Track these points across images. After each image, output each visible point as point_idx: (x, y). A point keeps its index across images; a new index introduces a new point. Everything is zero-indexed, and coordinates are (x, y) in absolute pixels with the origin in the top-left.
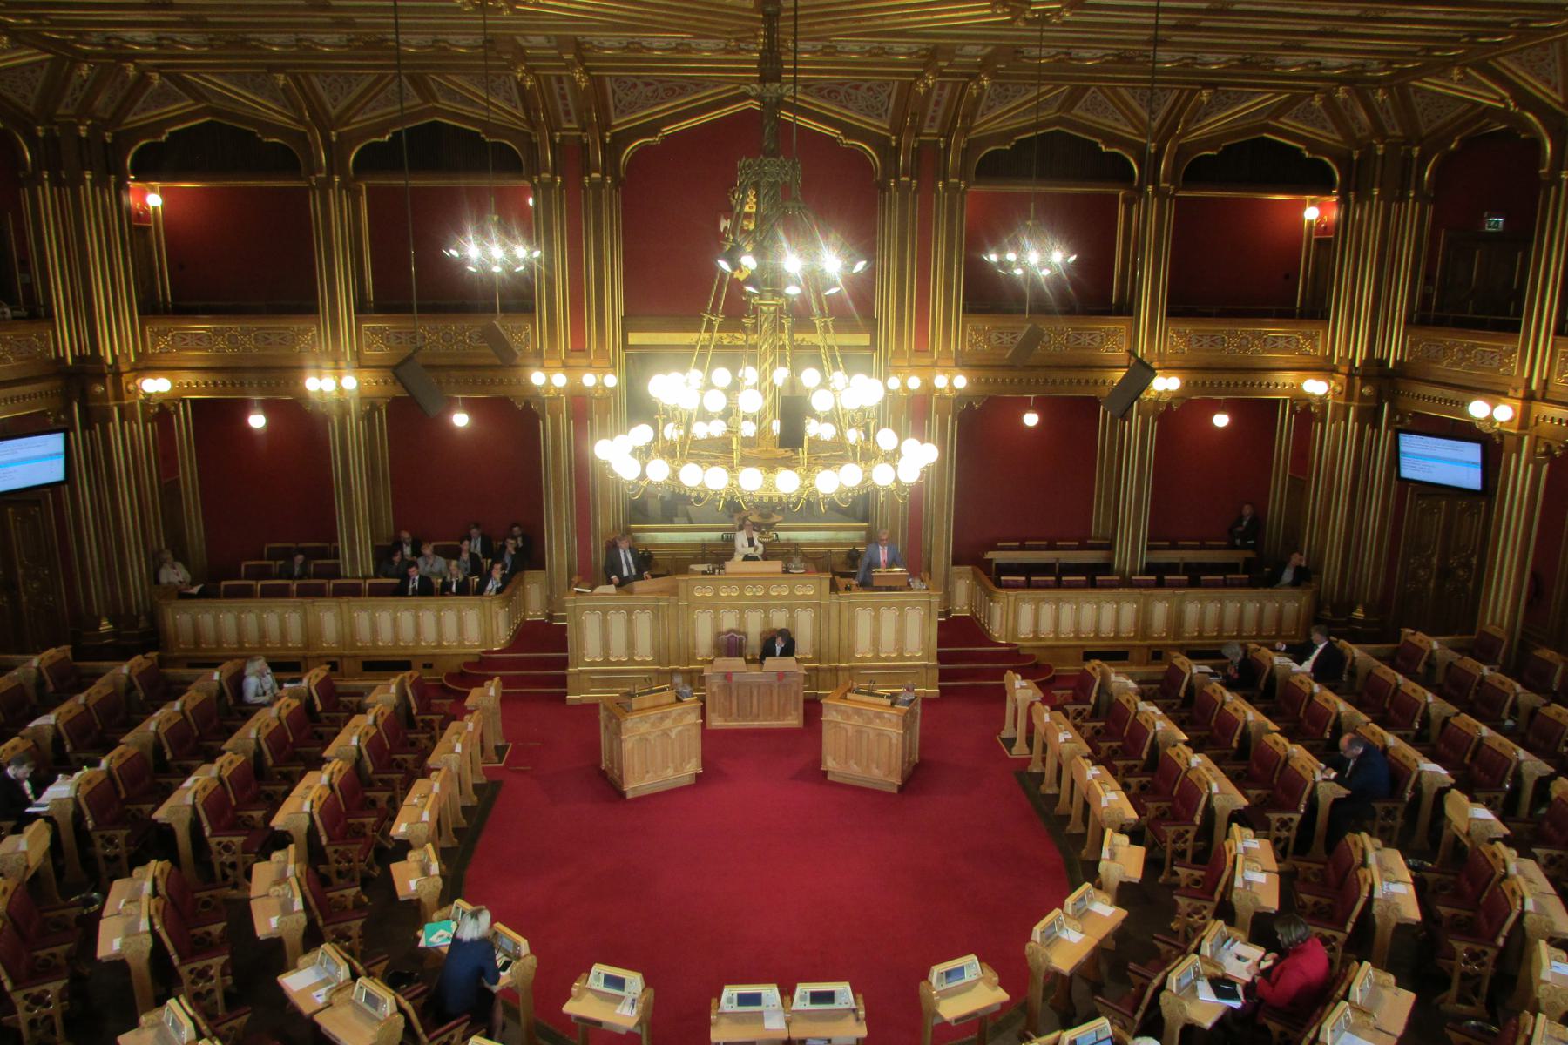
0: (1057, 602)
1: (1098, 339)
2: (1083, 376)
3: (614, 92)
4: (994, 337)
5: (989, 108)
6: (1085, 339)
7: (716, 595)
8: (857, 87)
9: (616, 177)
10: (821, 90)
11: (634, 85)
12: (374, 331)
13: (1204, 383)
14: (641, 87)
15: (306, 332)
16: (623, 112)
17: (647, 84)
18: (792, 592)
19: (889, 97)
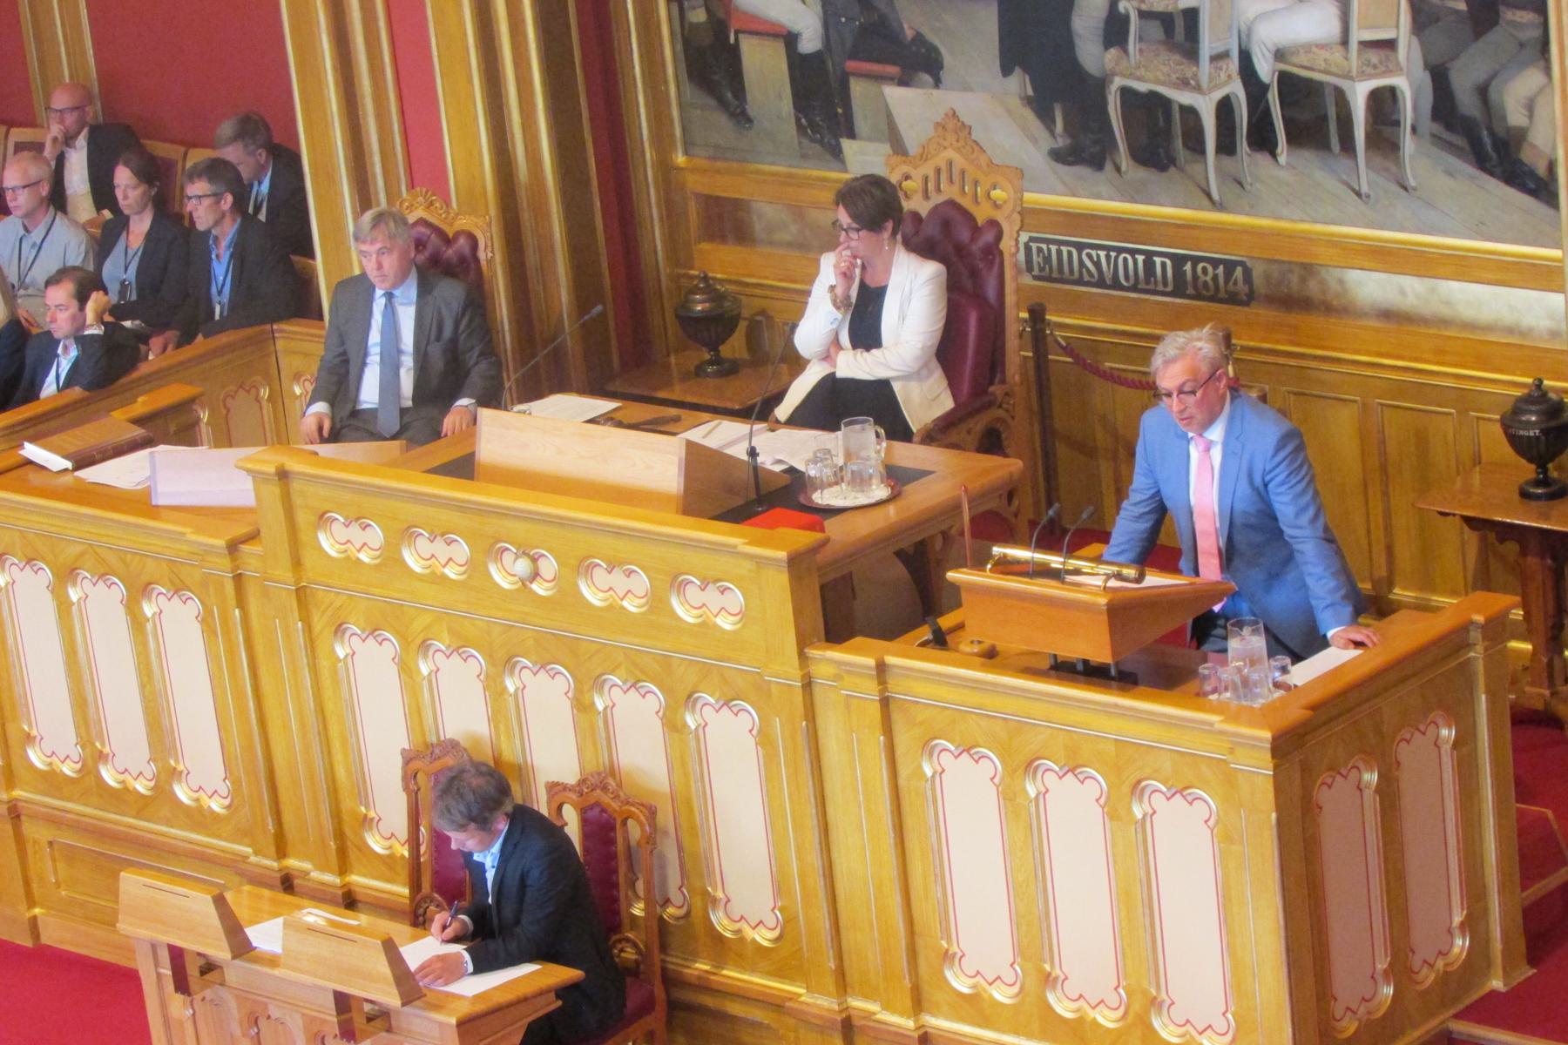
7: (390, 560)
18: (657, 602)
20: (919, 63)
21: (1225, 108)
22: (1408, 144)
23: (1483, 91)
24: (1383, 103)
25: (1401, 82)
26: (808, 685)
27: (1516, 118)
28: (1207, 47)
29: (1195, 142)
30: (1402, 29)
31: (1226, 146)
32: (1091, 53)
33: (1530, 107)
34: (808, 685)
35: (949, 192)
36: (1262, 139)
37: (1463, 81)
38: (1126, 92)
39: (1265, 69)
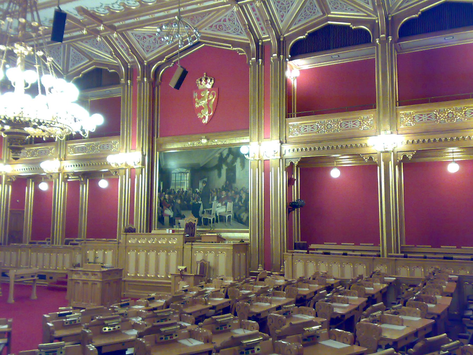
0: (317, 261)
1: (358, 124)
2: (349, 143)
3: (138, 42)
4: (302, 129)
5: (282, 16)
6: (350, 125)
8: (225, 20)
9: (149, 78)
10: (216, 26)
11: (144, 38)
12: (71, 147)
13: (424, 141)
14: (148, 38)
15: (51, 149)
16: (148, 51)
17: (150, 36)
19: (237, 21)
20: (183, 217)
21: (214, 219)
22: (231, 220)
23: (239, 215)
24: (229, 217)
25: (231, 215)
26: (183, 247)
27: (242, 217)
28: (212, 213)
29: (210, 222)
30: (232, 210)
31: (213, 222)
32: (200, 215)
33: (244, 216)
34: (183, 247)
35: (191, 221)
36: (217, 221)
37: (237, 214)
38: (204, 218)
39: (218, 215)
